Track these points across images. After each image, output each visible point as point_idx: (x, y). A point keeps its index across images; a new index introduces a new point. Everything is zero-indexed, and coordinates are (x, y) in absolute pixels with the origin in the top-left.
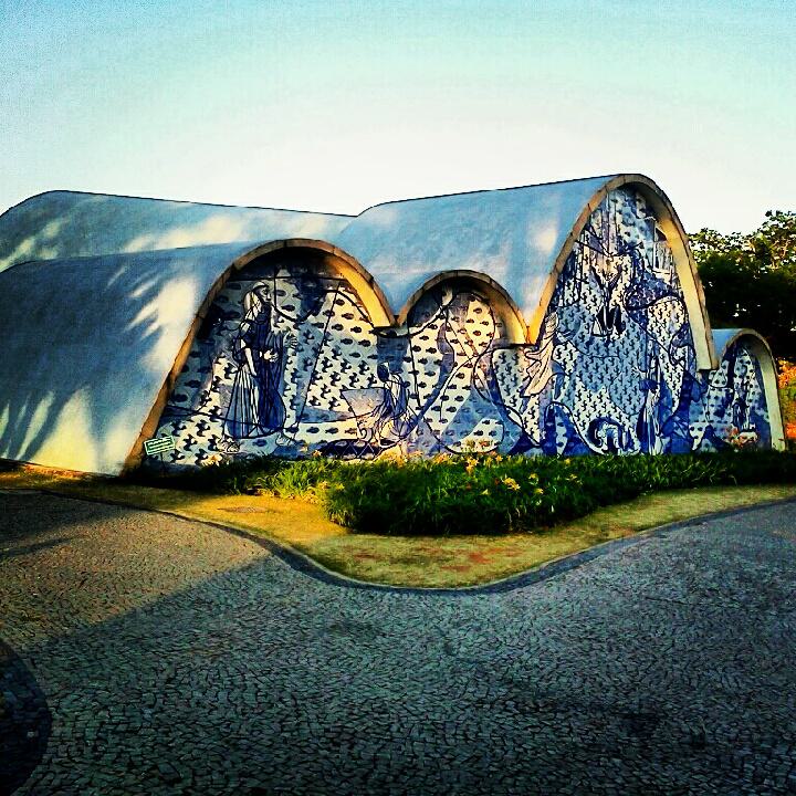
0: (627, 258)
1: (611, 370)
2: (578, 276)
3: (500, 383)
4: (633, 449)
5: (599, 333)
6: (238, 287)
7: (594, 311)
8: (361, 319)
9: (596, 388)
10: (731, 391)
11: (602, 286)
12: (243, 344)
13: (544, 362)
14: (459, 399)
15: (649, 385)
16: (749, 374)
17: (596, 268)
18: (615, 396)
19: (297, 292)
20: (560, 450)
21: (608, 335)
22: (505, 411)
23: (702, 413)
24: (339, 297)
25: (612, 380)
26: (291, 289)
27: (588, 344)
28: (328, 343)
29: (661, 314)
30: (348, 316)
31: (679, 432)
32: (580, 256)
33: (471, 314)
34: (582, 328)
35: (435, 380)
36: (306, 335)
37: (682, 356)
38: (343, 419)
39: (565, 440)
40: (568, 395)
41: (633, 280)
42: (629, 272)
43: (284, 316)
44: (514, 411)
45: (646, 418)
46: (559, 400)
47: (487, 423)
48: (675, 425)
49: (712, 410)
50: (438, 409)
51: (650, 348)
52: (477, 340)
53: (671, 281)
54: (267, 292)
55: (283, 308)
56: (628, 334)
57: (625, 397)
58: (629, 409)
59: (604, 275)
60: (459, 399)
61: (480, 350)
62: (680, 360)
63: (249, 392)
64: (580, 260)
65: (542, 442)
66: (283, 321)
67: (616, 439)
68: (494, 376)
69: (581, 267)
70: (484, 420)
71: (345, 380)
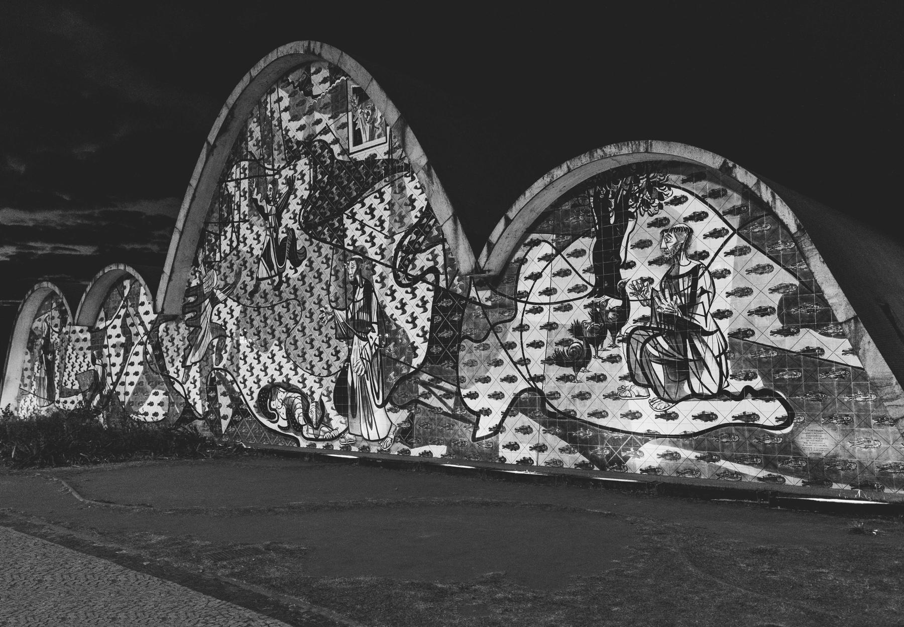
0: (302, 165)
1: (287, 320)
2: (236, 218)
3: (165, 355)
4: (328, 425)
5: (265, 275)
7: (257, 252)
9: (265, 346)
10: (615, 303)
11: (266, 217)
13: (203, 326)
14: (136, 374)
15: (359, 328)
16: (698, 244)
17: (259, 197)
18: (293, 353)
20: (225, 424)
21: (279, 274)
22: (170, 381)
23: (498, 363)
25: (288, 332)
27: (252, 294)
29: (372, 210)
31: (433, 402)
32: (237, 194)
34: (245, 277)
35: (119, 360)
37: (431, 264)
38: (76, 393)
39: (229, 412)
40: (231, 359)
41: (312, 188)
42: (307, 178)
44: (178, 382)
45: (352, 378)
46: (221, 366)
47: (156, 394)
48: (421, 389)
49: (537, 356)
50: (123, 384)
51: (351, 271)
52: (147, 319)
53: (390, 152)
56: (311, 262)
57: (310, 354)
58: (319, 367)
59: (268, 202)
60: (136, 374)
61: (149, 327)
62: (424, 273)
63: (44, 378)
64: (237, 200)
65: (206, 414)
67: (299, 412)
68: (161, 350)
69: (239, 207)
70: (154, 391)
71: (77, 368)
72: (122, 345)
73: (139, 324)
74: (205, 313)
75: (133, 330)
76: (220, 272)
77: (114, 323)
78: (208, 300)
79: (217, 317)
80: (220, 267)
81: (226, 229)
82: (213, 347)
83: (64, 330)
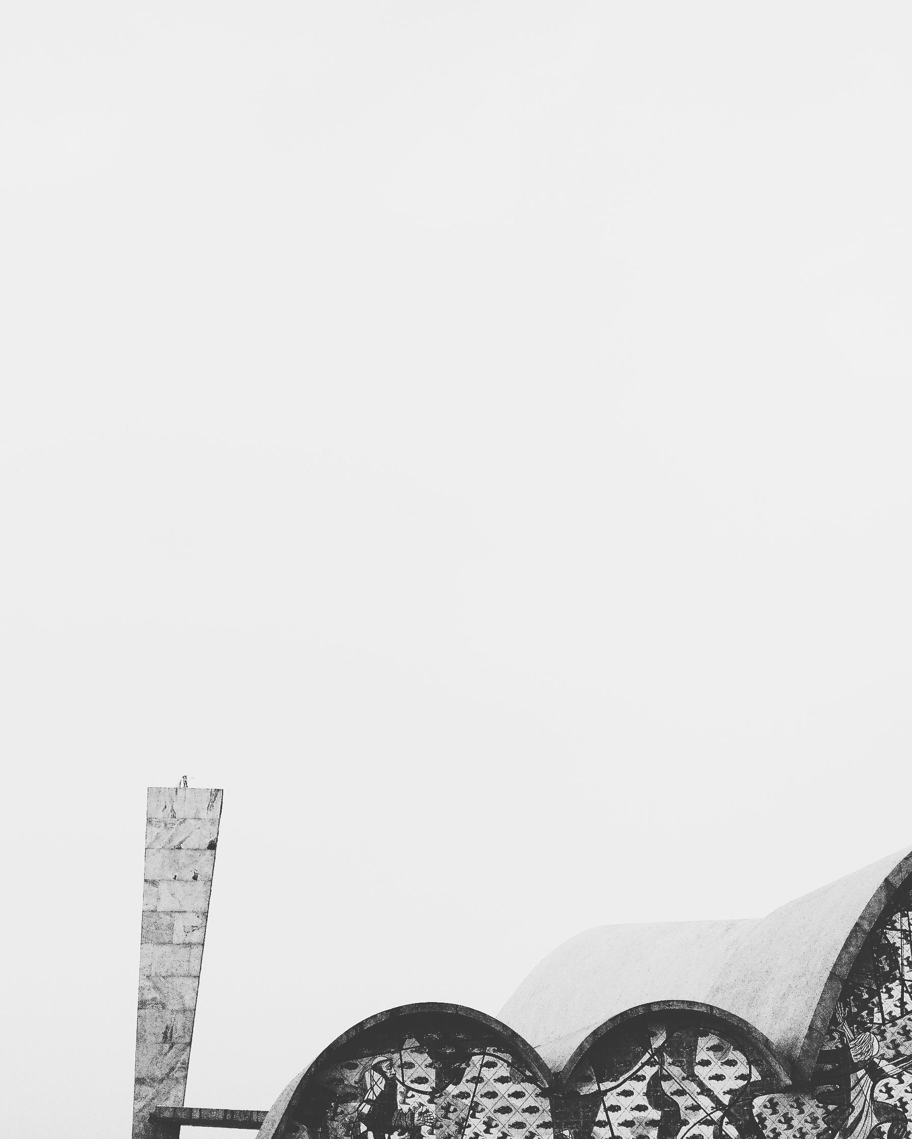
6: (355, 1067)
8: (523, 1081)
12: (363, 1128)
13: (858, 1104)
19: (429, 1061)
24: (487, 1058)
26: (423, 1059)
28: (477, 1115)
30: (503, 1080)
33: (701, 1055)
36: (446, 1109)
43: (413, 1090)
52: (718, 1088)
54: (391, 1066)
55: (412, 1082)
61: (726, 1099)
66: (413, 1096)
72: (652, 1123)
73: (699, 1094)
74: (858, 1088)
75: (683, 1102)
76: (884, 1038)
77: (627, 1086)
78: (862, 1072)
79: (886, 1095)
80: (885, 1031)
81: (890, 986)
82: (884, 1133)
83: (452, 1089)
